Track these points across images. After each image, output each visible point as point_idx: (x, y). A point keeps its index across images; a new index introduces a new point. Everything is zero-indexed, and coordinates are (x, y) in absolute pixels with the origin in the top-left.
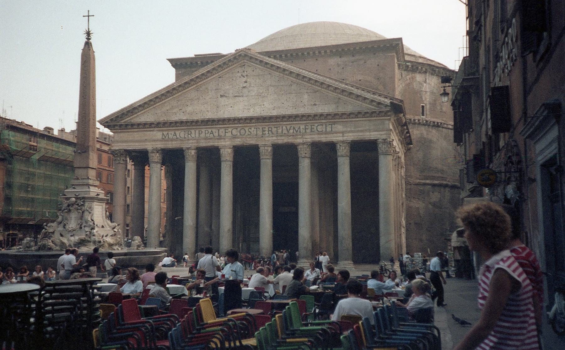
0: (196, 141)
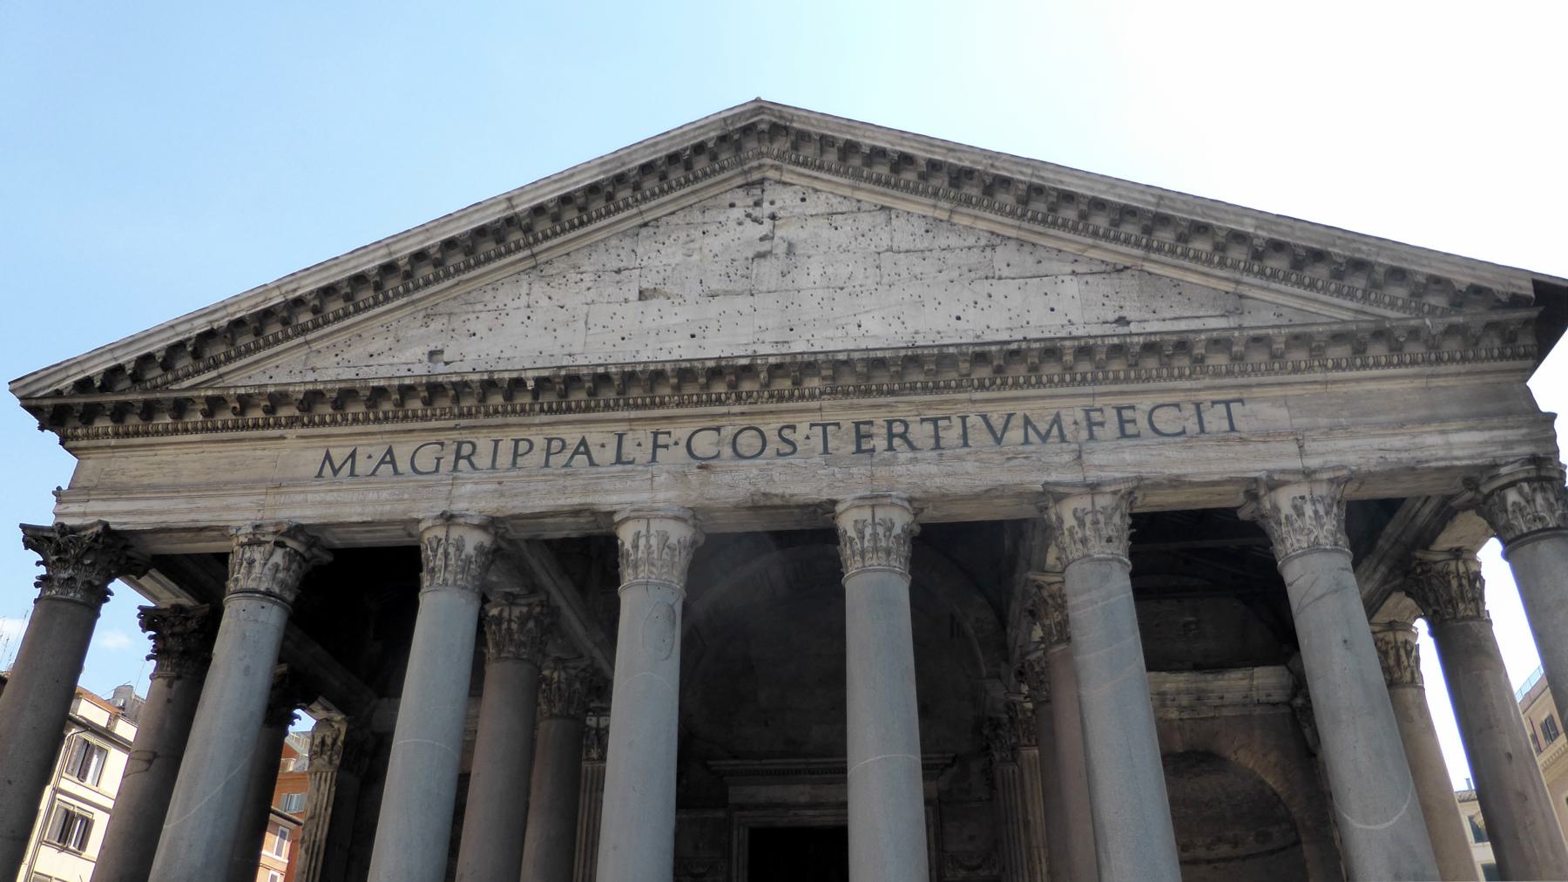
0: (497, 486)
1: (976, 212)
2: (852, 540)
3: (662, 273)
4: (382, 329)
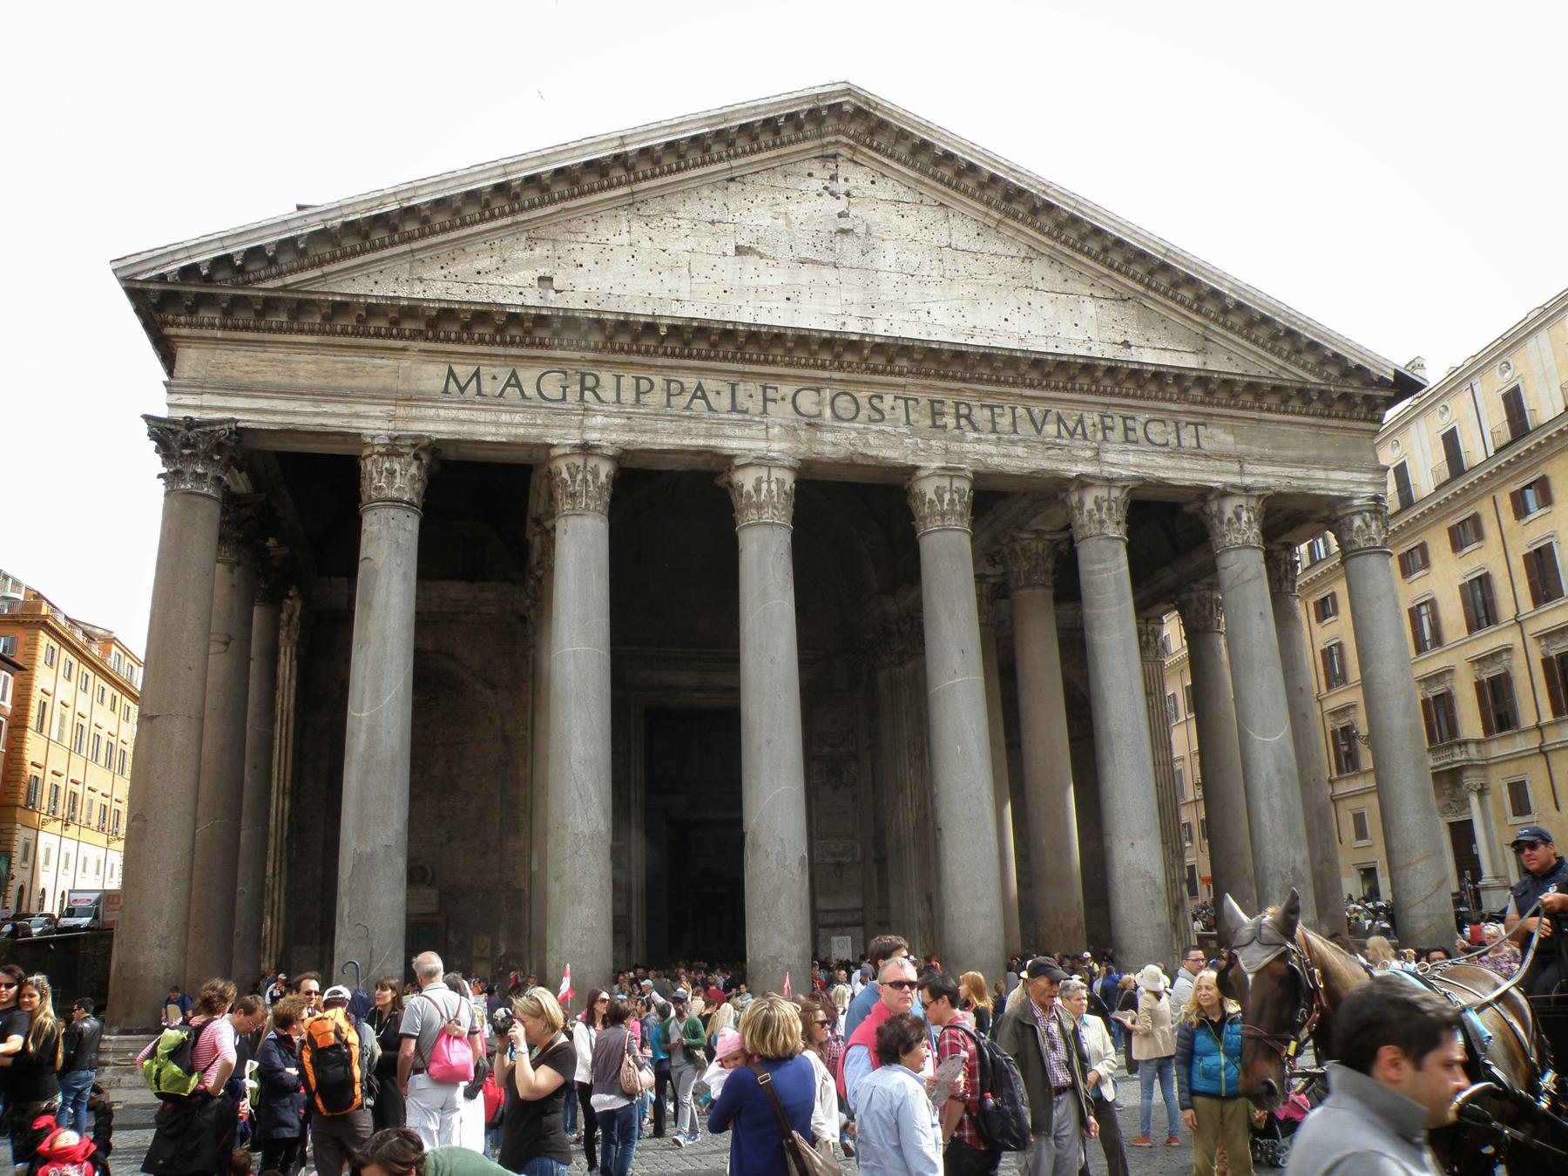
0: (625, 421)
1: (1020, 226)
2: (931, 502)
3: (756, 233)
4: (483, 246)
